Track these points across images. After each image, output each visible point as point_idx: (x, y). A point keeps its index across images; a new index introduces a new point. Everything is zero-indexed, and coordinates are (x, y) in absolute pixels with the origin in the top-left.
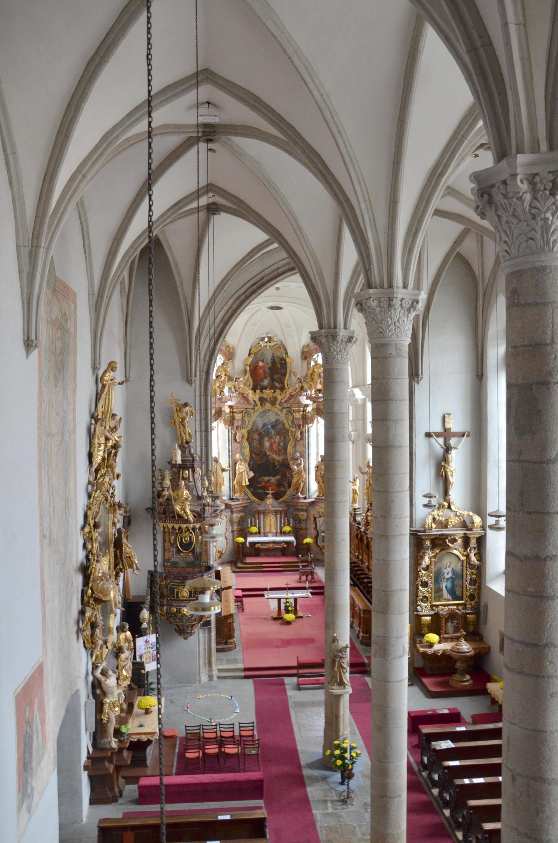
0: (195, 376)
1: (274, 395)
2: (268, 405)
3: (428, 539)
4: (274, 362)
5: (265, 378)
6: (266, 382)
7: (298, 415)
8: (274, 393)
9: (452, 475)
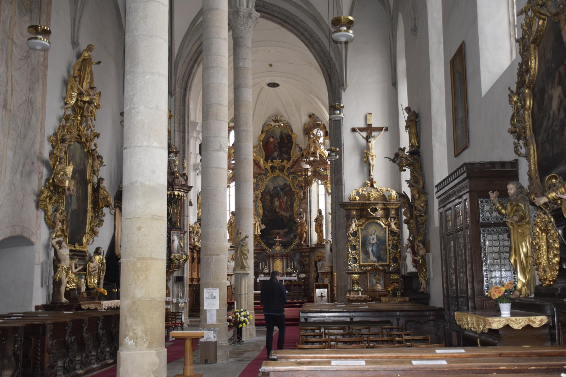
0: (175, 90)
1: (283, 164)
3: (354, 209)
4: (281, 136)
5: (275, 150)
6: (276, 154)
7: (302, 179)
8: (282, 162)
9: (372, 159)
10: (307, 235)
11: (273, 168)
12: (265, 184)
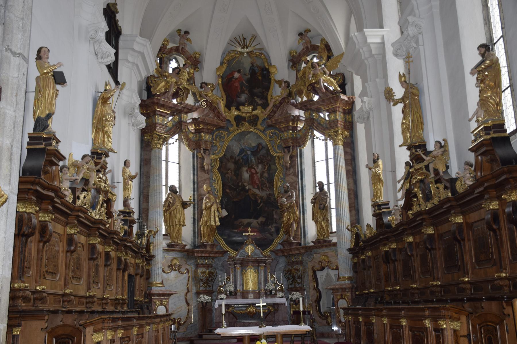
1: (255, 112)
2: (246, 127)
4: (253, 72)
5: (243, 92)
6: (243, 97)
8: (253, 110)
10: (299, 226)
11: (239, 120)
12: (226, 144)
